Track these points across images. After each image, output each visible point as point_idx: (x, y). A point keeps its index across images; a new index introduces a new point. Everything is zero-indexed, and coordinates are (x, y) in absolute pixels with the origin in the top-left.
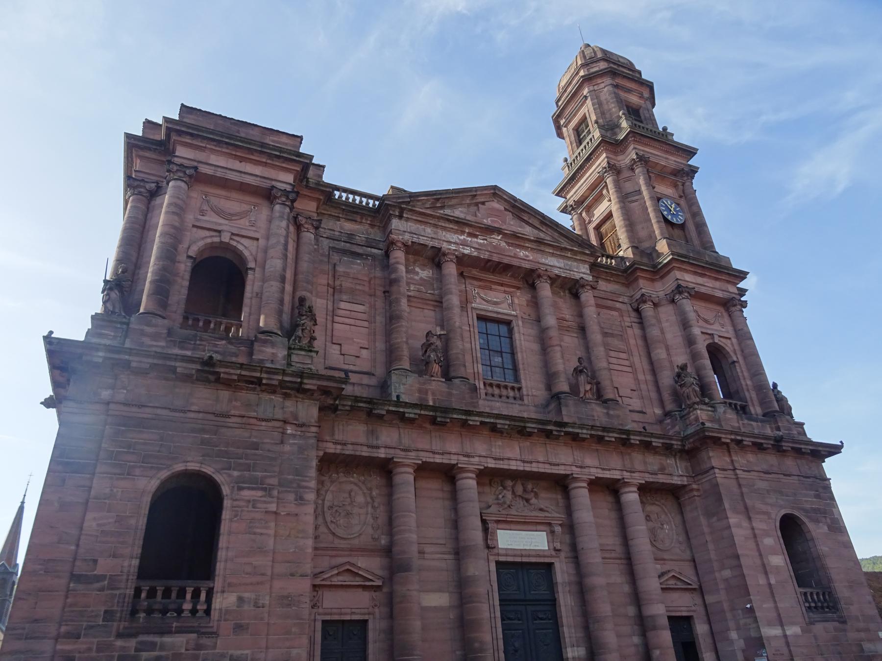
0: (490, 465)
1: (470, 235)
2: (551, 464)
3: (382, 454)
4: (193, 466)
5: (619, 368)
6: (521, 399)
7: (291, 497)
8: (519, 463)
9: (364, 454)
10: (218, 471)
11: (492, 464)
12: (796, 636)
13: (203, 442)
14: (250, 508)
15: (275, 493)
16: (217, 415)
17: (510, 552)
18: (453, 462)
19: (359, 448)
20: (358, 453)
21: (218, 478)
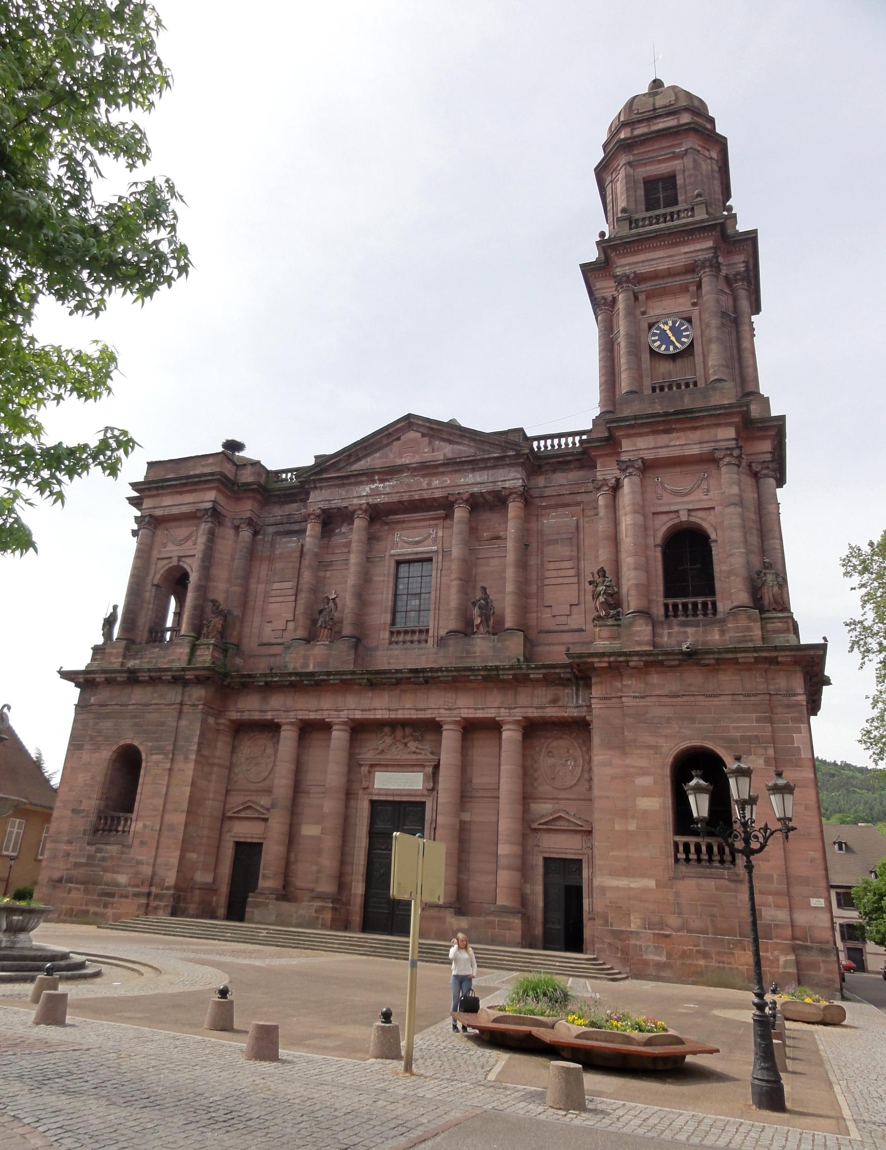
0: (357, 717)
1: (382, 481)
2: (417, 710)
3: (269, 716)
4: (128, 741)
5: (560, 581)
6: (426, 641)
7: (181, 758)
8: (384, 712)
9: (256, 718)
10: (141, 744)
11: (358, 715)
12: (645, 890)
15: (170, 756)
17: (382, 792)
18: (324, 717)
19: (253, 713)
21: (141, 748)
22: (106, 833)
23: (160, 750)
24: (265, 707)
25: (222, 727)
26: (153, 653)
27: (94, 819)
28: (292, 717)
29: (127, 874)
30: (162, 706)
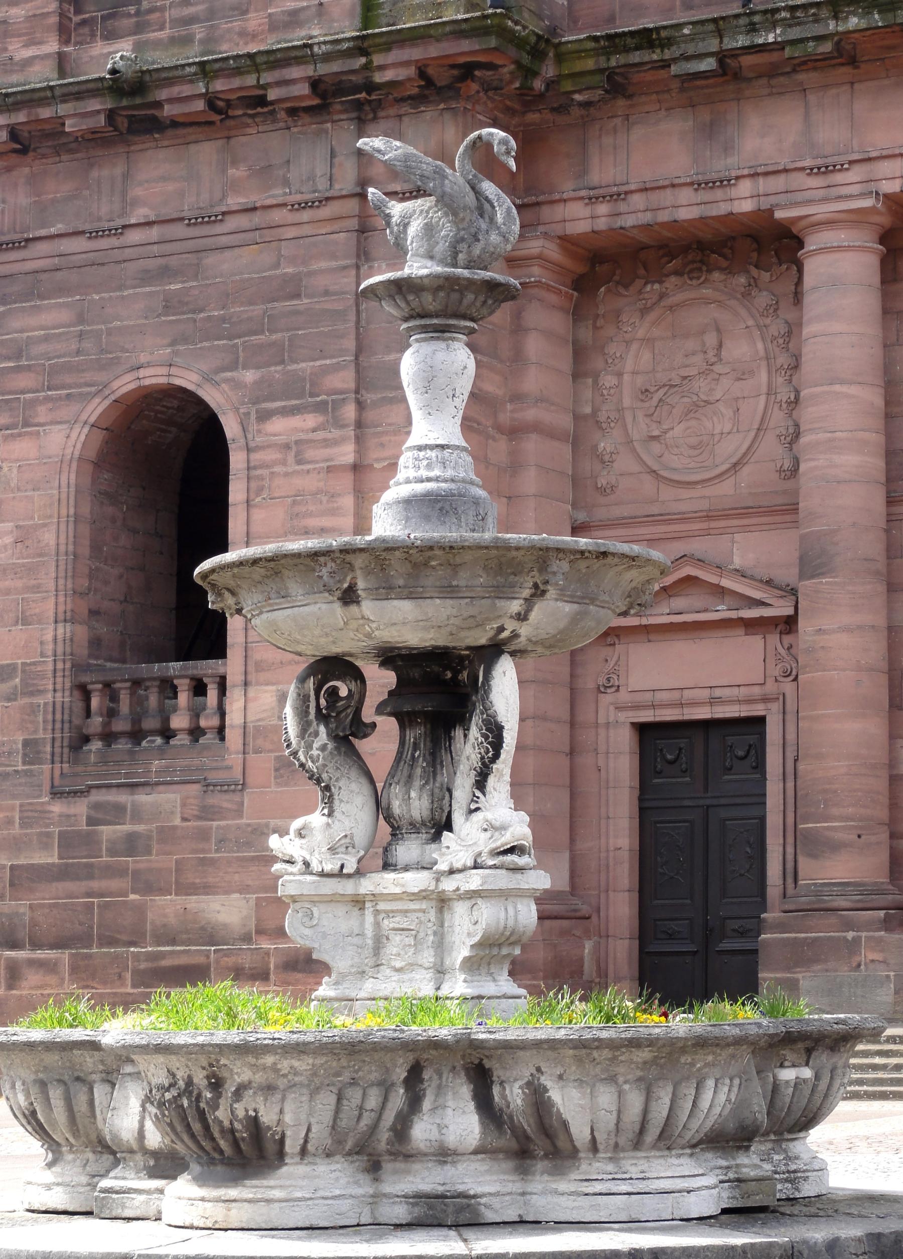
3: (743, 200)
4: (153, 377)
9: (684, 214)
13: (169, 305)
14: (293, 467)
16: (193, 222)
19: (667, 197)
20: (664, 217)
21: (212, 397)
22: (122, 745)
23: (300, 395)
24: (720, 165)
25: (536, 273)
27: (64, 698)
28: (855, 192)
29: (244, 889)
30: (277, 216)
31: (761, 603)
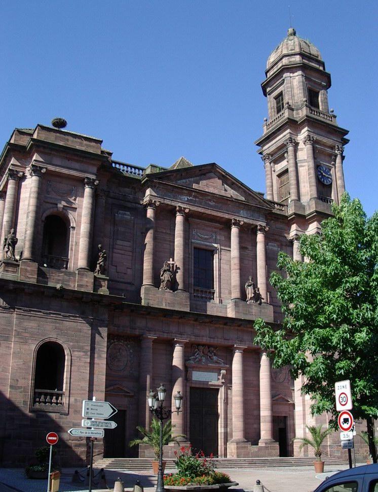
3: (137, 332)
4: (53, 340)
21: (65, 346)
26: (59, 276)
31: (128, 393)
